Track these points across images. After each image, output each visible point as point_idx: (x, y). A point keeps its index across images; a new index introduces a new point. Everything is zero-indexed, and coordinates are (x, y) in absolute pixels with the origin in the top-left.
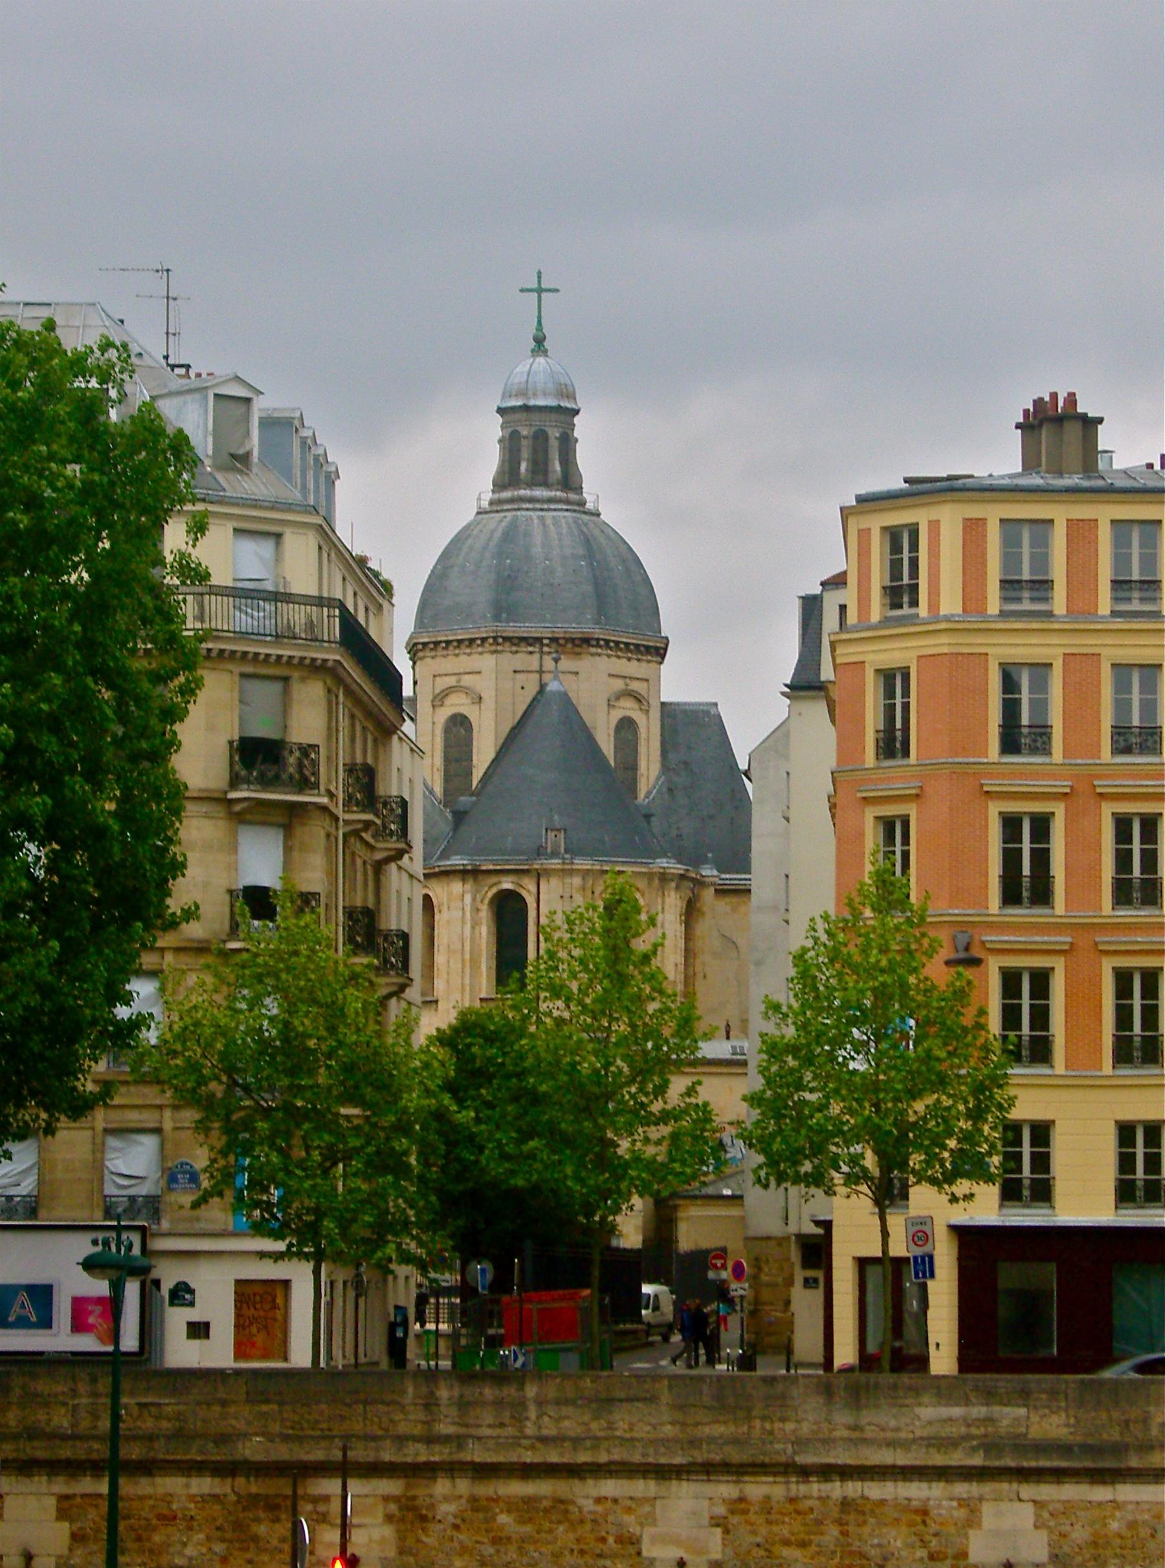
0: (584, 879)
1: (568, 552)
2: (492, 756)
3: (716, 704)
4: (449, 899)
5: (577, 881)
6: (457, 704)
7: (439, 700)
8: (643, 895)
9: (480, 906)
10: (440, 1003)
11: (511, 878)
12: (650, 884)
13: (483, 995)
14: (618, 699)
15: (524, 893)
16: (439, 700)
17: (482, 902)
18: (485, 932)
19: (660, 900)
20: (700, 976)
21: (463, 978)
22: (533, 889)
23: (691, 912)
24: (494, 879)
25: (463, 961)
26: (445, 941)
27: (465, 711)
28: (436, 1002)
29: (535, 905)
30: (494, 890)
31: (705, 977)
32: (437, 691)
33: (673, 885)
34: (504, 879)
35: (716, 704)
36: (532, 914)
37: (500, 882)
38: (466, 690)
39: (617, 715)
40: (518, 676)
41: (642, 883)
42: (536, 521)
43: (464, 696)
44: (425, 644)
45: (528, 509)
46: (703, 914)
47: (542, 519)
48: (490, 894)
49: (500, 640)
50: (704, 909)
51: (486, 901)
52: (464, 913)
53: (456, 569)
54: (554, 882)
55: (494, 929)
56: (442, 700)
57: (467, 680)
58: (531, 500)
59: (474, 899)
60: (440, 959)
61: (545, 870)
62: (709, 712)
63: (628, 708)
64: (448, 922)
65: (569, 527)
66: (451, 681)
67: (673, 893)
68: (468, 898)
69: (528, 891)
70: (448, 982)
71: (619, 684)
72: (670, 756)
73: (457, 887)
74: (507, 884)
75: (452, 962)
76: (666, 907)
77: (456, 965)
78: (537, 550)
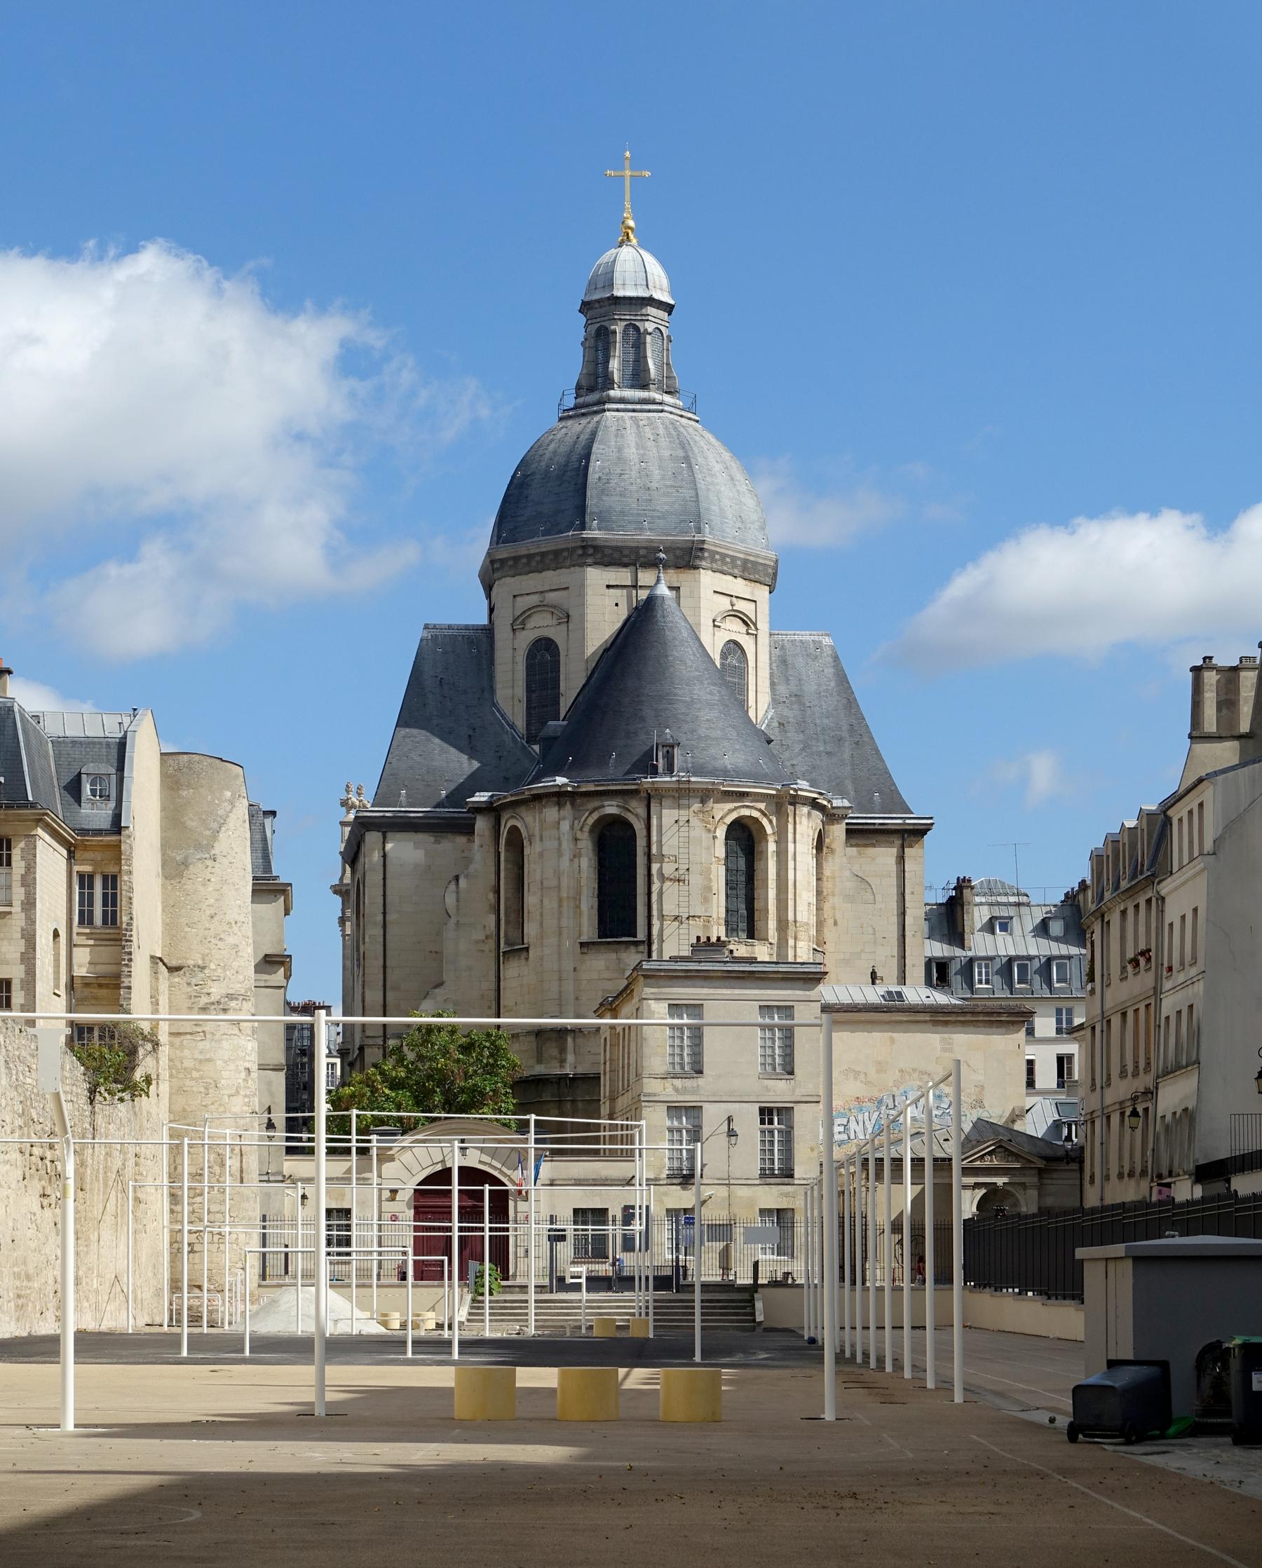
1: (666, 453)
2: (584, 682)
4: (541, 829)
6: (542, 625)
7: (519, 623)
9: (579, 835)
10: (531, 952)
13: (584, 939)
15: (631, 818)
16: (519, 623)
17: (581, 829)
18: (587, 865)
21: (559, 919)
22: (641, 811)
23: (820, 844)
25: (560, 900)
26: (538, 877)
27: (550, 633)
28: (527, 949)
29: (645, 832)
30: (595, 816)
31: (835, 923)
32: (518, 613)
36: (641, 843)
38: (553, 608)
39: (722, 637)
40: (612, 591)
42: (628, 423)
43: (549, 616)
44: (503, 561)
45: (618, 410)
47: (635, 420)
48: (591, 821)
49: (590, 551)
51: (587, 829)
52: (560, 844)
55: (594, 863)
56: (523, 623)
57: (552, 597)
58: (622, 401)
59: (572, 827)
60: (531, 900)
61: (657, 789)
62: (820, 642)
63: (734, 630)
64: (541, 855)
65: (666, 428)
66: (534, 600)
67: (804, 820)
68: (565, 826)
69: (636, 815)
70: (541, 924)
71: (725, 603)
73: (551, 813)
74: (611, 808)
75: (546, 902)
77: (550, 904)
78: (631, 453)
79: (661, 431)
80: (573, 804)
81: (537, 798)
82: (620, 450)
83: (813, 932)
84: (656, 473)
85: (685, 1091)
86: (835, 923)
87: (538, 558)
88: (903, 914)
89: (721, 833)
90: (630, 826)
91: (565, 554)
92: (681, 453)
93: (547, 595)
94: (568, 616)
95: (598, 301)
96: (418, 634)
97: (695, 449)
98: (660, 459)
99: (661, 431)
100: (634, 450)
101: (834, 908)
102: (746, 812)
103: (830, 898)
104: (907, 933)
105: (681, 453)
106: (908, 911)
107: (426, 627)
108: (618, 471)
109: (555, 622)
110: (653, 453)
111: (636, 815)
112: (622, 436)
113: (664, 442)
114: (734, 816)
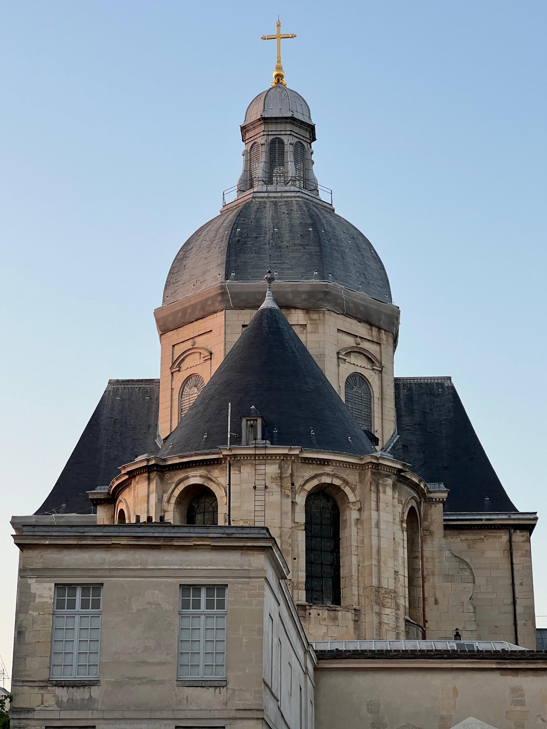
0: (280, 468)
1: (297, 222)
3: (449, 378)
5: (272, 469)
8: (353, 490)
11: (201, 471)
12: (361, 481)
14: (348, 354)
15: (213, 487)
17: (168, 501)
19: (373, 495)
20: (430, 601)
22: (223, 480)
23: (413, 521)
24: (181, 475)
29: (226, 500)
30: (181, 487)
31: (436, 602)
33: (390, 481)
34: (192, 473)
35: (449, 378)
37: (187, 478)
39: (347, 370)
41: (352, 477)
42: (268, 204)
46: (431, 534)
48: (177, 493)
50: (432, 528)
51: (173, 500)
53: (194, 249)
54: (247, 470)
59: (160, 500)
62: (442, 384)
63: (358, 364)
67: (389, 491)
68: (153, 499)
69: (218, 484)
71: (350, 341)
72: (406, 420)
74: (195, 478)
76: (382, 505)
79: (295, 208)
80: (162, 478)
81: (132, 474)
82: (258, 220)
83: (403, 602)
84: (287, 236)
85: (72, 705)
86: (436, 602)
87: (189, 310)
88: (514, 603)
89: (301, 499)
90: (210, 494)
91: (209, 303)
92: (309, 221)
93: (196, 339)
94: (211, 354)
95: (252, 124)
96: (103, 387)
97: (324, 221)
98: (292, 226)
99: (295, 208)
100: (270, 221)
101: (434, 588)
102: (327, 480)
103: (431, 578)
104: (519, 622)
105: (309, 221)
106: (518, 601)
107: (110, 382)
108: (255, 235)
109: (202, 360)
110: (286, 221)
111: (218, 484)
112: (262, 212)
113: (296, 214)
114: (315, 482)
